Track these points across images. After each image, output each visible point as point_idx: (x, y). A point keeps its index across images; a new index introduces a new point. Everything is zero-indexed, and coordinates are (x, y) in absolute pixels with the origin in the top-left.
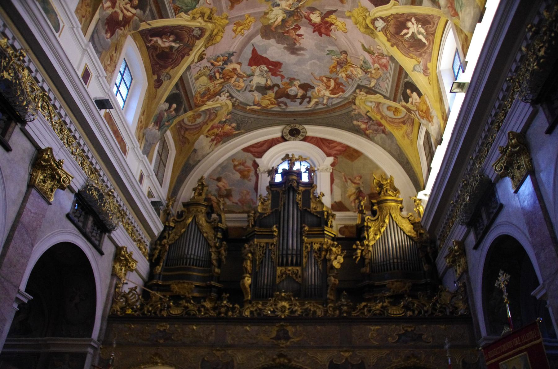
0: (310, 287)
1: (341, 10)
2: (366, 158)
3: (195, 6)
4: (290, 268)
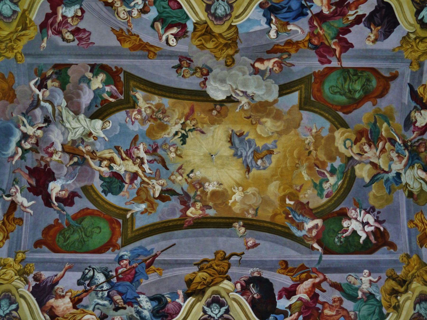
1: (409, 78)
3: (377, 300)
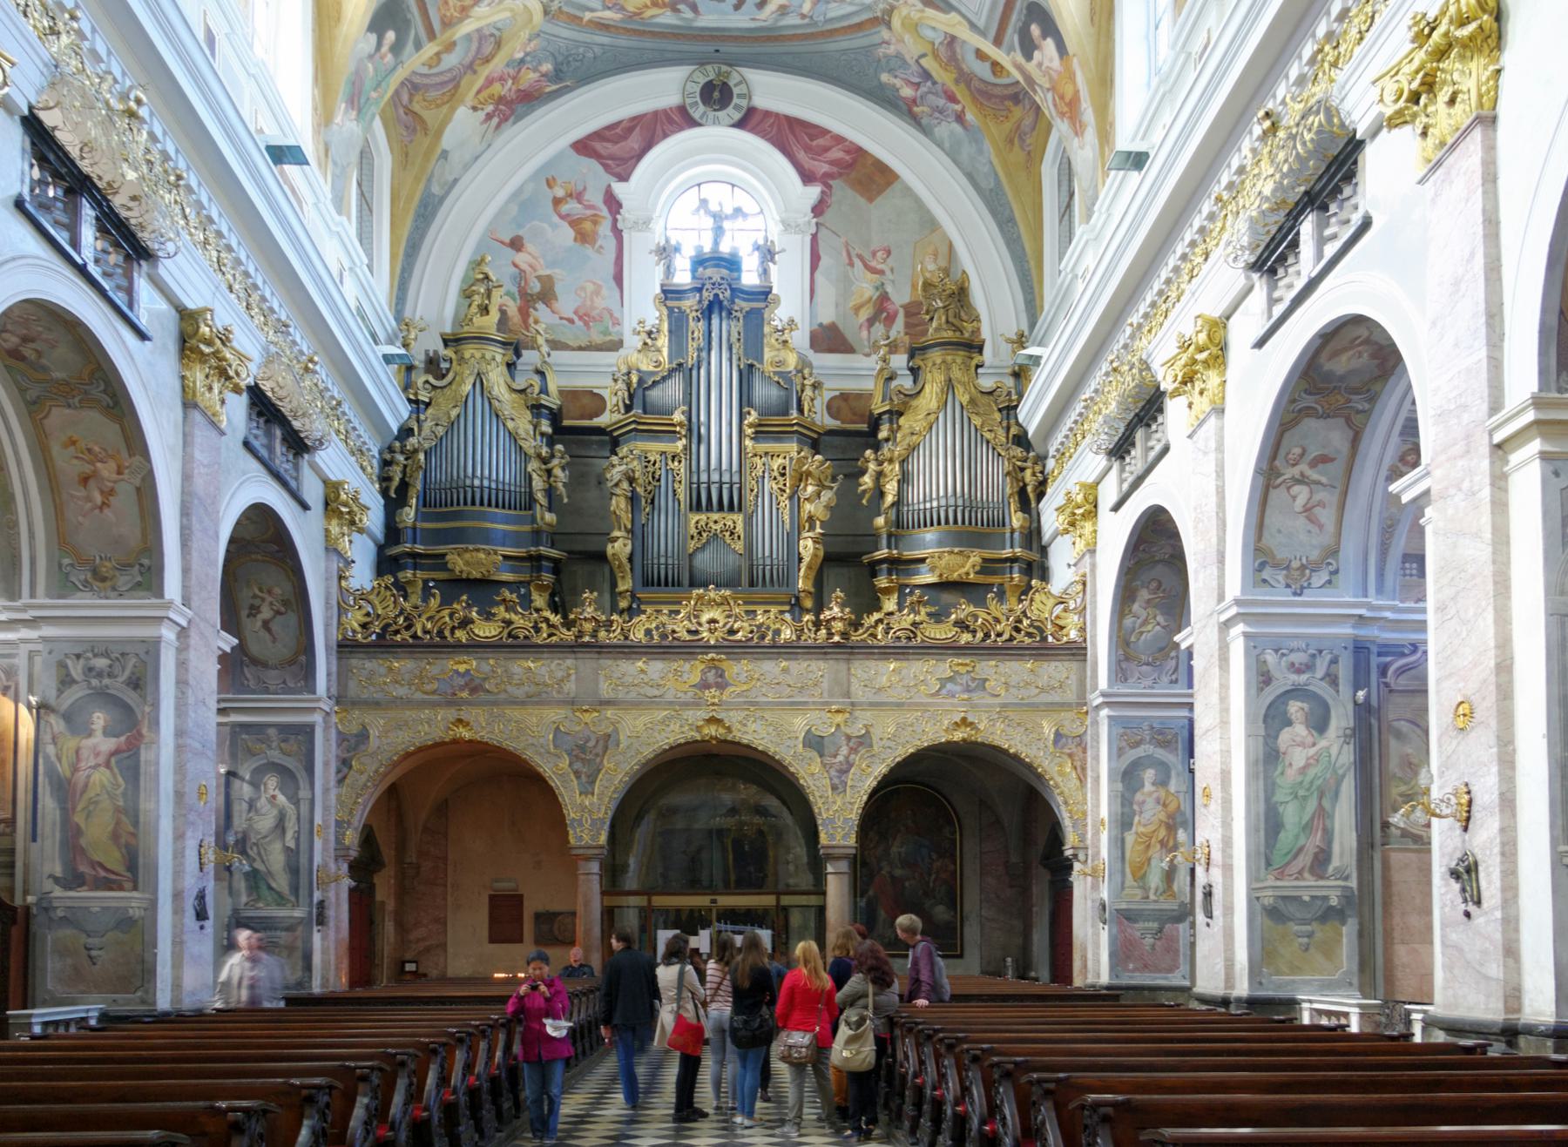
2: (908, 191)
4: (715, 516)
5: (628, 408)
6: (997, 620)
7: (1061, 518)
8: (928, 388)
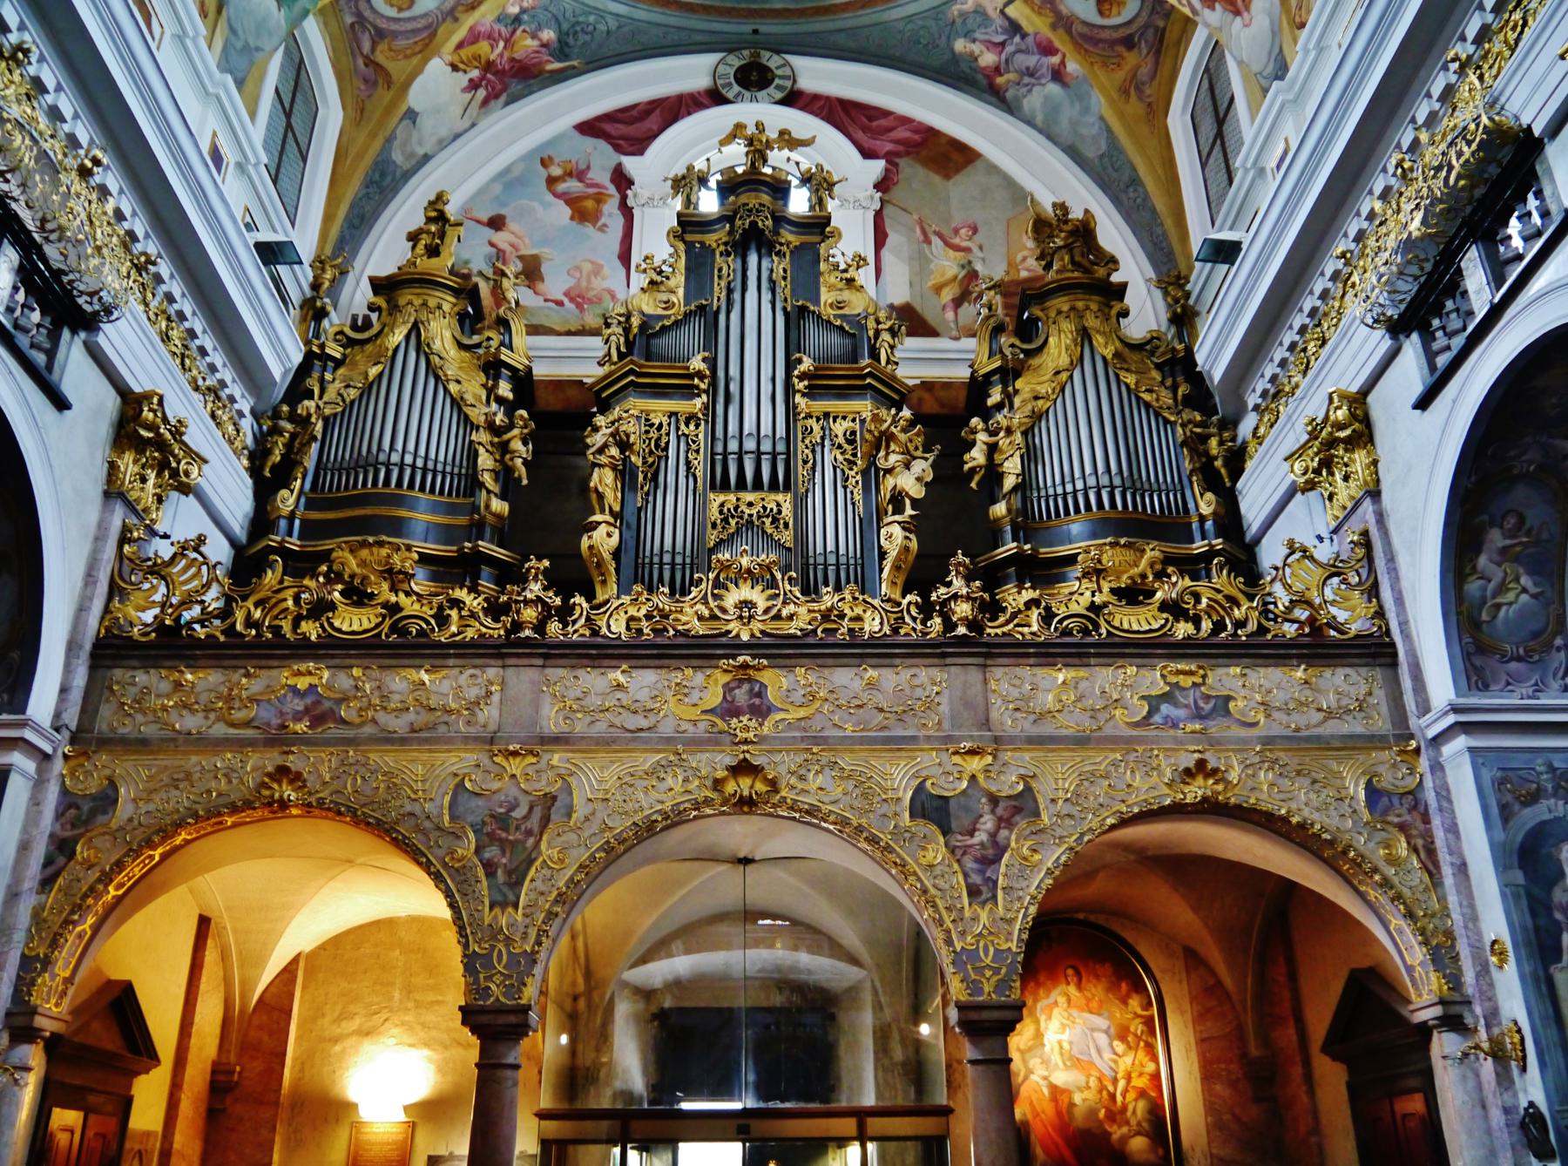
0: (820, 560)
2: (993, 169)
4: (749, 497)
5: (621, 356)
6: (1234, 602)
7: (1298, 467)
8: (1051, 340)
